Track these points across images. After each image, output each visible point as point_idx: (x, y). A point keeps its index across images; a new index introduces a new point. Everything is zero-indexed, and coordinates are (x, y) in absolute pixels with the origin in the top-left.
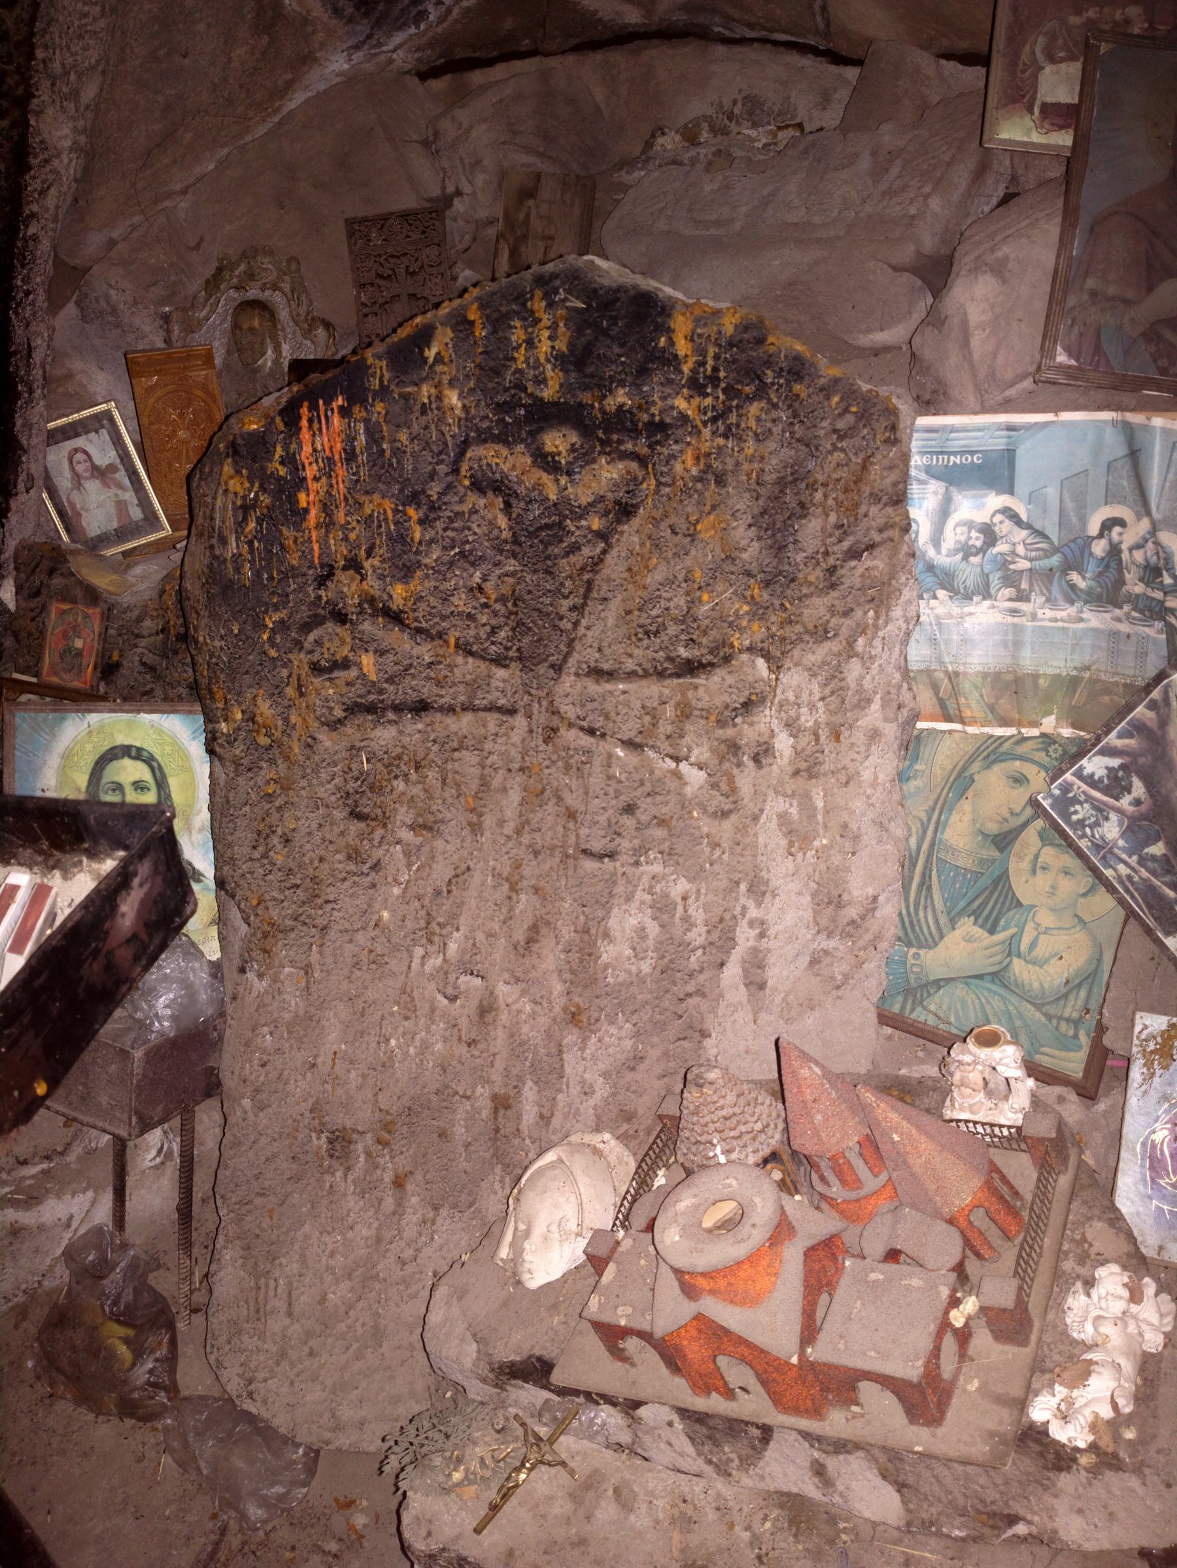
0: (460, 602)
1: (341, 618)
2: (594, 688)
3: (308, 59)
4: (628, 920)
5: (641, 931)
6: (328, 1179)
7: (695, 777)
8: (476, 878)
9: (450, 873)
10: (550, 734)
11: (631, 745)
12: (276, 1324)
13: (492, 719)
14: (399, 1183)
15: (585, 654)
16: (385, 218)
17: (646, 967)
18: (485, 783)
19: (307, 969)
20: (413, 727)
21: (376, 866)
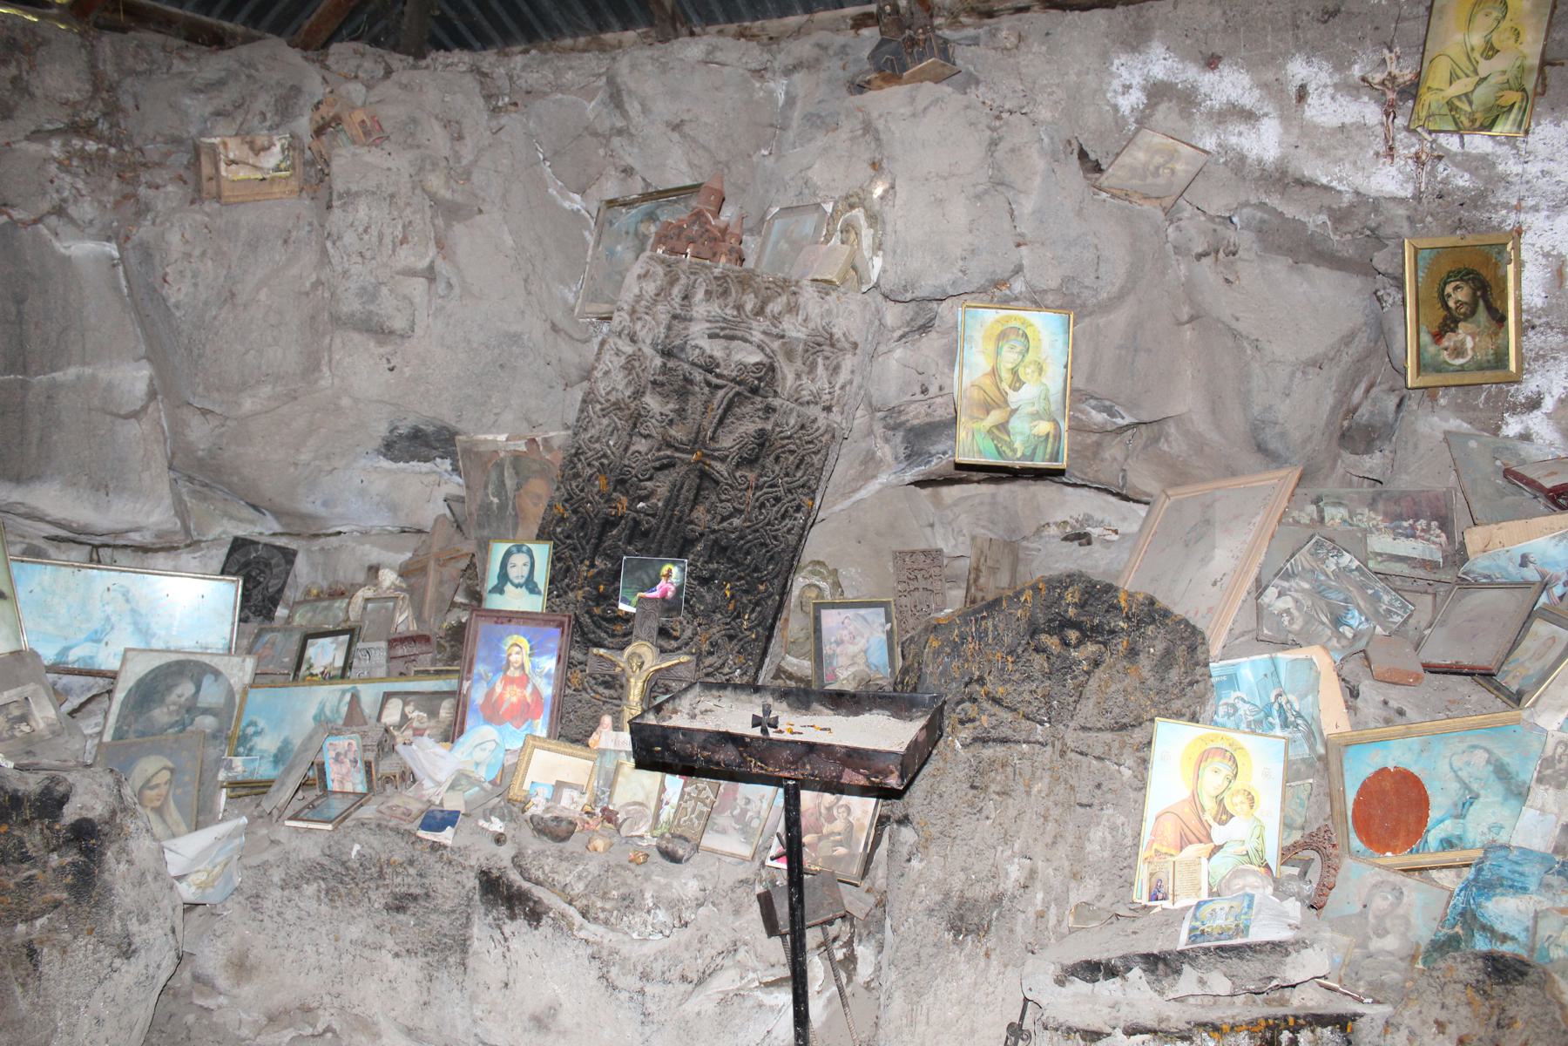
0: (1027, 696)
1: (974, 700)
2: (1082, 734)
3: (874, 477)
4: (1097, 834)
5: (1104, 840)
6: (952, 956)
7: (1127, 773)
8: (1027, 817)
9: (1015, 813)
10: (1063, 754)
11: (1099, 758)
12: (921, 1028)
13: (1037, 747)
14: (987, 955)
15: (1079, 720)
16: (913, 553)
17: (1106, 854)
18: (1033, 774)
19: (945, 857)
20: (1000, 750)
21: (980, 811)
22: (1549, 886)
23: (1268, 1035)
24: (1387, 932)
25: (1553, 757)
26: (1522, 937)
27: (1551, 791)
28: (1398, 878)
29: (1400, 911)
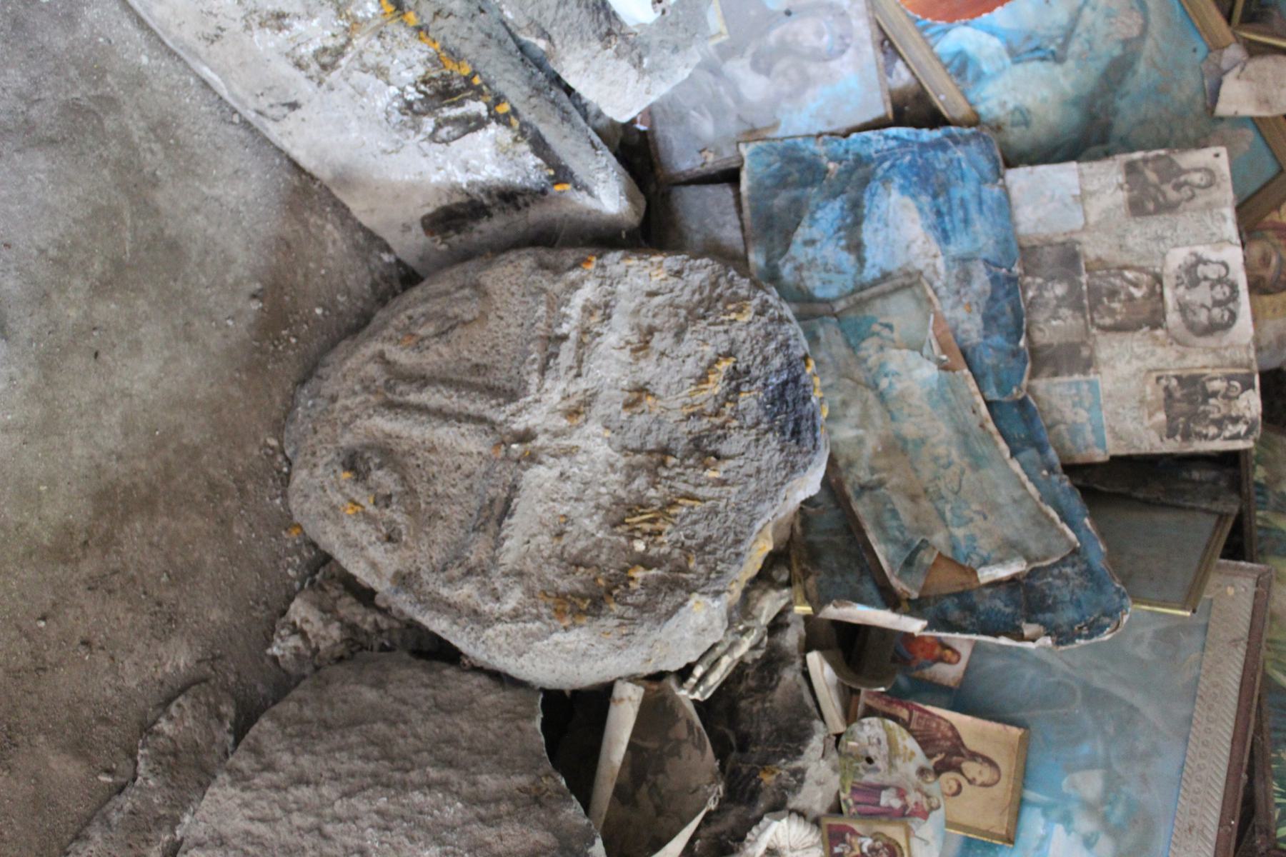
22: (966, 278)
23: (457, 84)
24: (767, 72)
25: (1182, 172)
26: (870, 273)
27: (1122, 196)
28: (862, 30)
29: (813, 69)
